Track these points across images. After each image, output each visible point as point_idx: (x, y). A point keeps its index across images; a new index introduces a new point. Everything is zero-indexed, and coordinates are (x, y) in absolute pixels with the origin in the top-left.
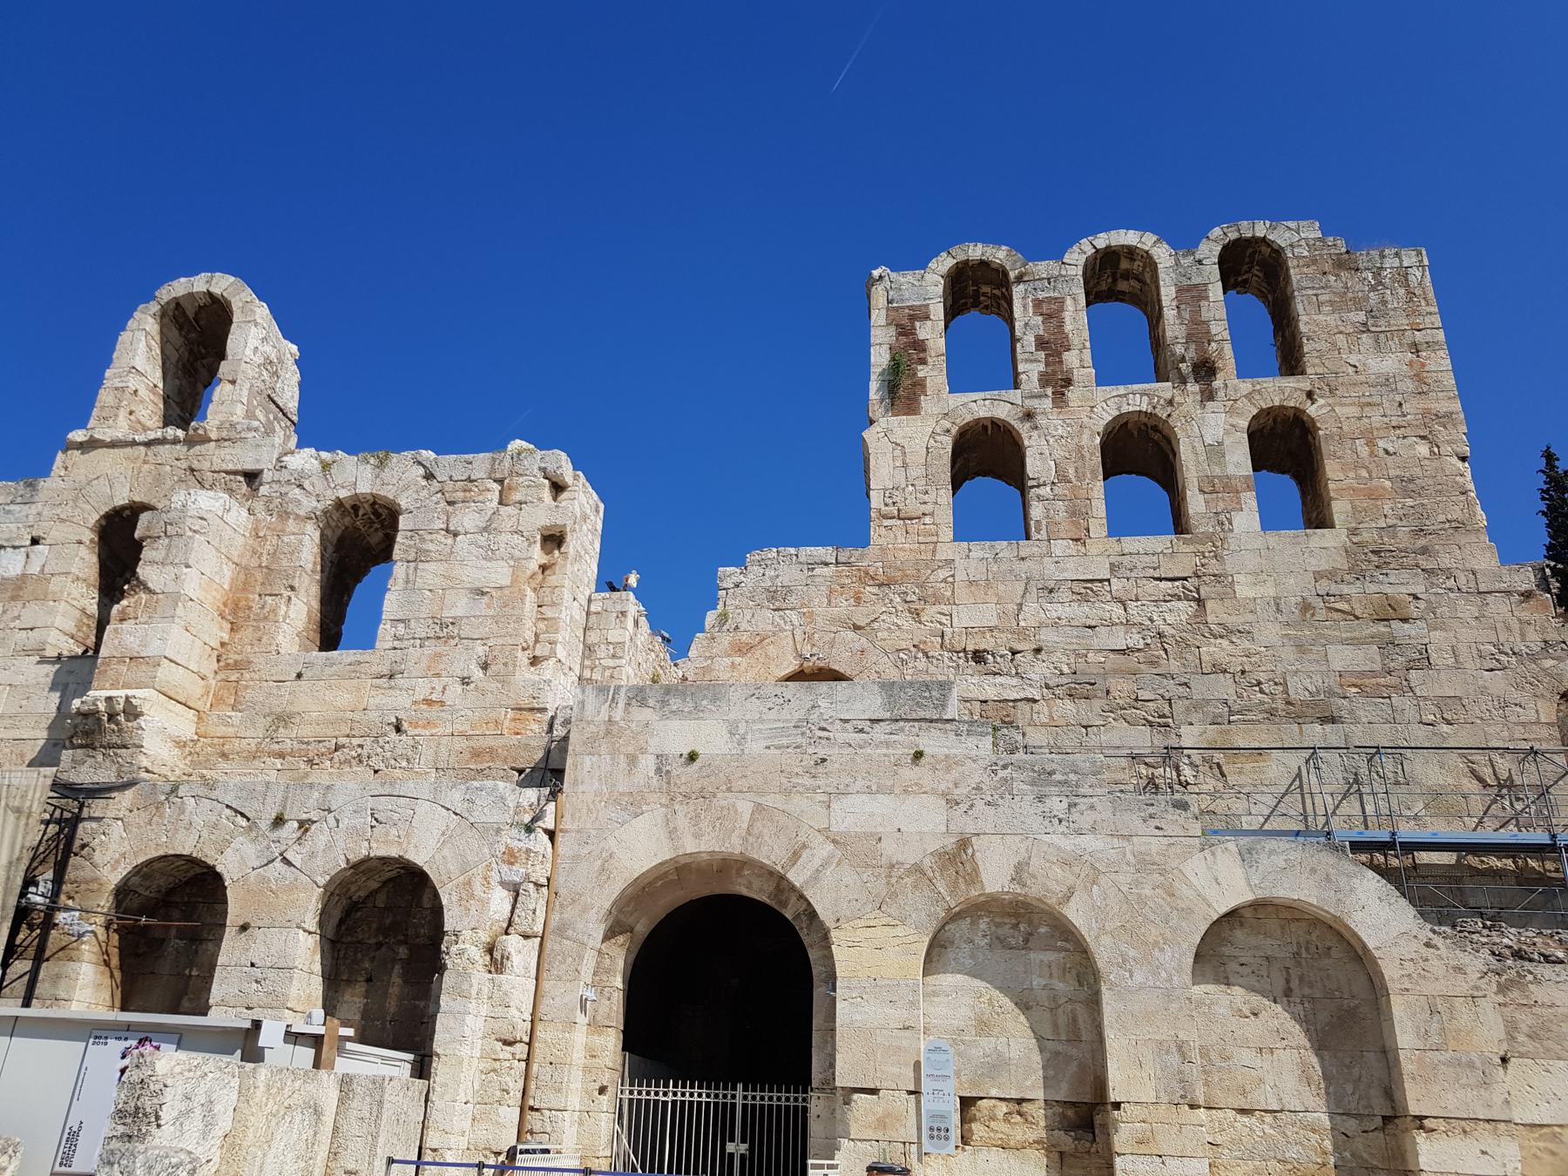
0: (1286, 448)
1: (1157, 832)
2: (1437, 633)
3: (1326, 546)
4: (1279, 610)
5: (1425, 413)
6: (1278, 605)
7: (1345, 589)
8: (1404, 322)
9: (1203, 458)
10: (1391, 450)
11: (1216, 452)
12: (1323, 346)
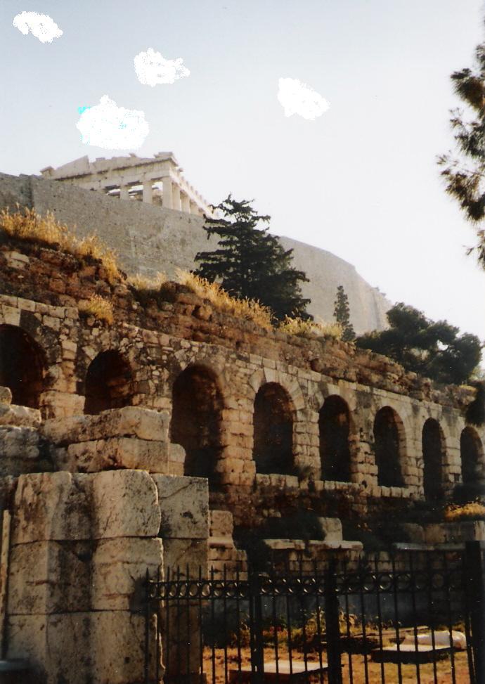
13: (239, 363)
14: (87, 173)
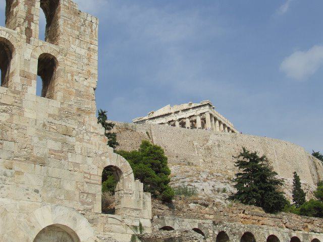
0: (47, 67)
1: (28, 200)
2: (78, 143)
3: (53, 105)
4: (36, 124)
5: (89, 71)
6: (36, 122)
7: (56, 122)
8: (88, 39)
9: (22, 63)
10: (77, 80)
11: (27, 62)
12: (66, 39)
13: (260, 229)
14: (170, 112)
